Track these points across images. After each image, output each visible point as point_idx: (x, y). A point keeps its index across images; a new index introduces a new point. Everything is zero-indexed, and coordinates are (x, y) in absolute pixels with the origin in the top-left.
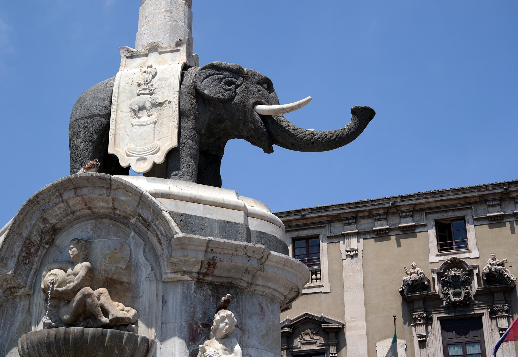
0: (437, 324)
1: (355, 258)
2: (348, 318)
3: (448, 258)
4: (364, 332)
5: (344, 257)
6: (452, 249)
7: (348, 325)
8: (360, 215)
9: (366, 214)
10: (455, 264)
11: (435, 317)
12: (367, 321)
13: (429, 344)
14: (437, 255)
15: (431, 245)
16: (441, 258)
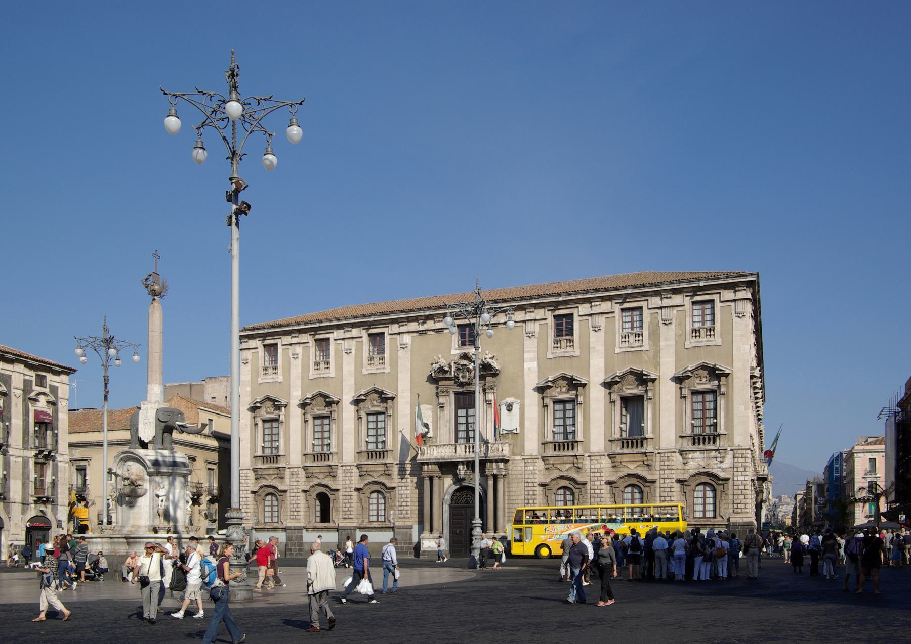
0: (453, 396)
1: (405, 349)
2: (400, 390)
3: (462, 351)
4: (409, 400)
5: (399, 349)
6: (466, 345)
7: (399, 395)
8: (411, 319)
9: (414, 318)
10: (465, 357)
11: (451, 391)
12: (411, 393)
13: (447, 408)
14: (456, 349)
15: (453, 343)
16: (458, 352)
